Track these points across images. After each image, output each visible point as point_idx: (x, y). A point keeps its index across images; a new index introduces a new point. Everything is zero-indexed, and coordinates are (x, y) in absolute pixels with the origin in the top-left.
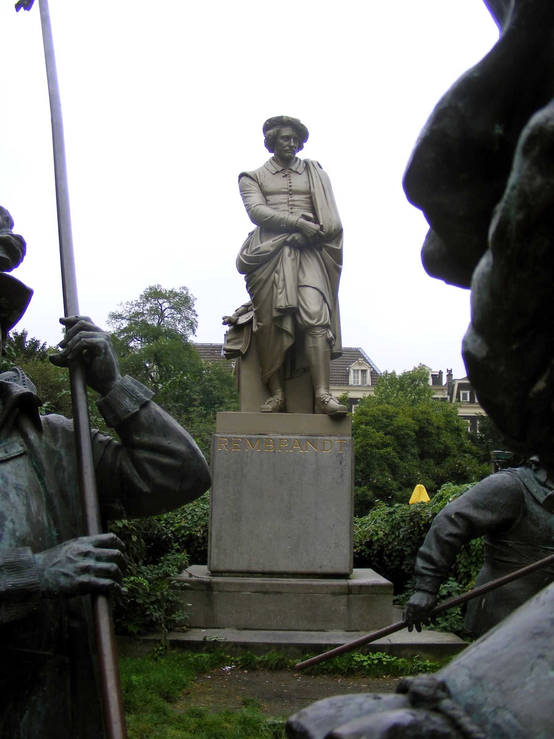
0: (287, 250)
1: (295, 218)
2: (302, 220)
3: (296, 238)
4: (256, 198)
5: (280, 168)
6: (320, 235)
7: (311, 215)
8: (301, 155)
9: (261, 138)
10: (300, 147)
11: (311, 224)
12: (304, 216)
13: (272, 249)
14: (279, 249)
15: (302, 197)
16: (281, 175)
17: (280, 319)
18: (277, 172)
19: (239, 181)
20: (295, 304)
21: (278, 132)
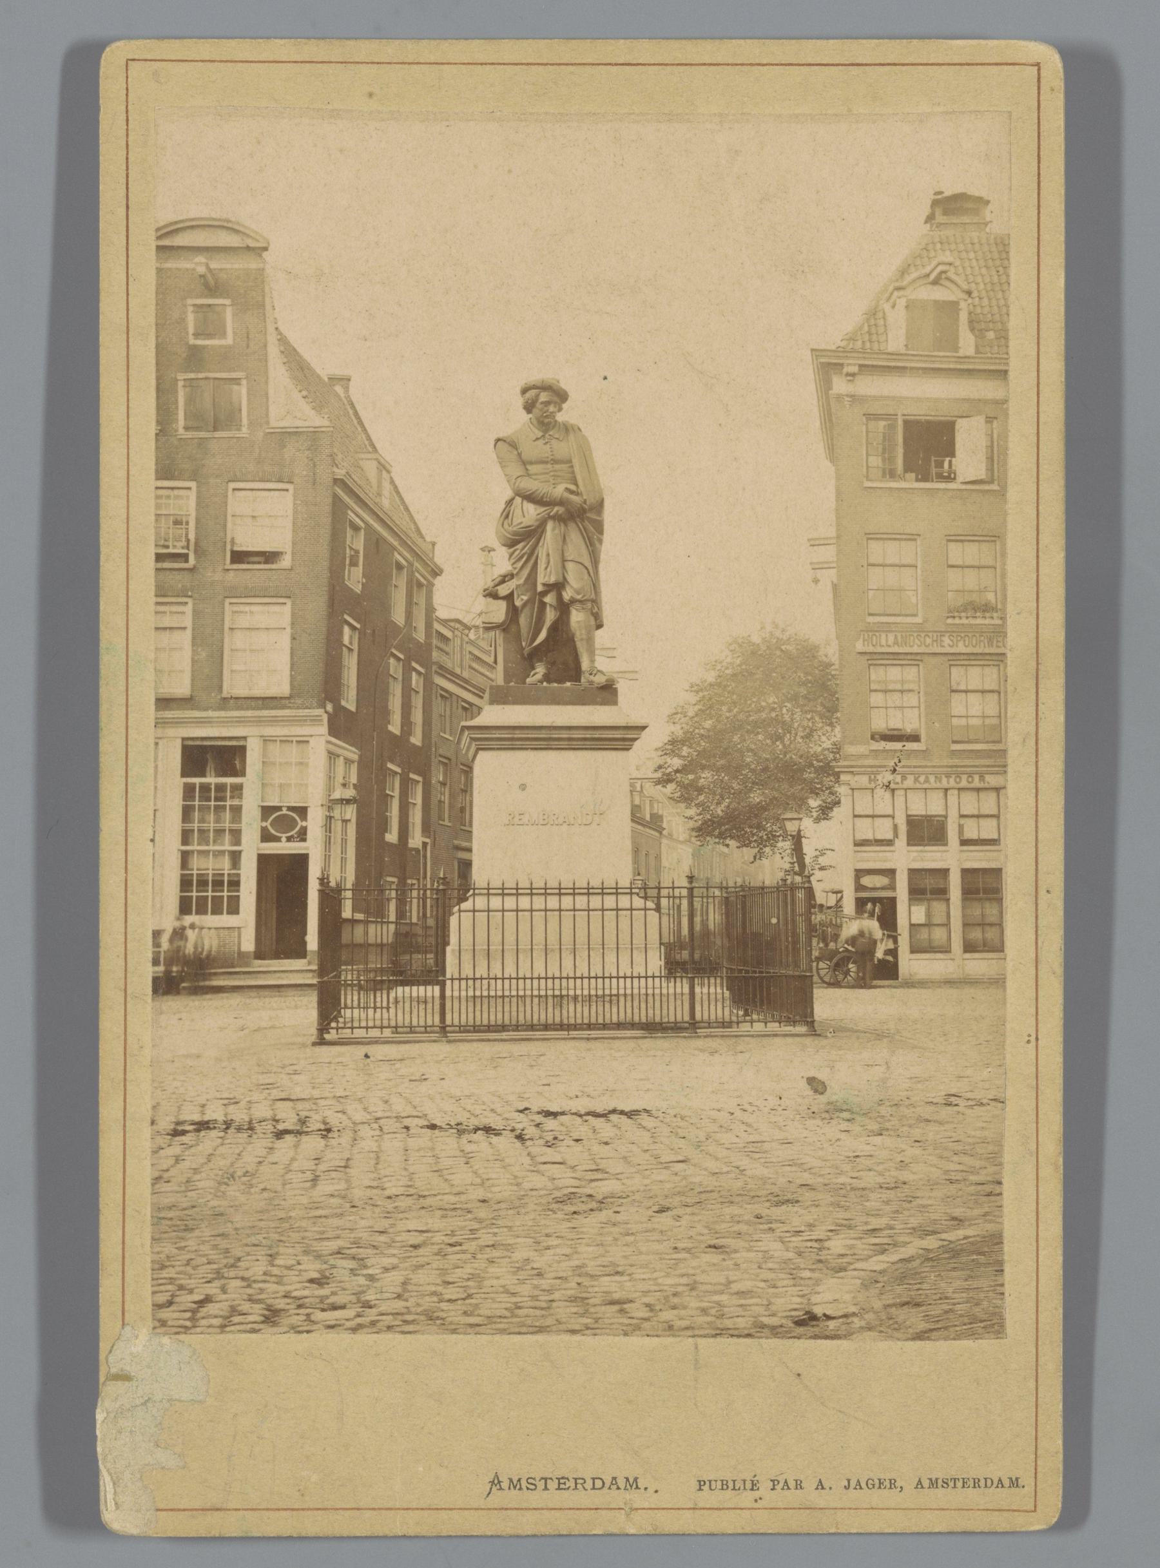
0: (550, 525)
1: (559, 491)
2: (566, 495)
3: (560, 512)
4: (516, 470)
5: (540, 434)
6: (582, 507)
7: (573, 487)
8: (560, 417)
9: (519, 401)
10: (560, 410)
11: (573, 497)
12: (567, 489)
13: (537, 524)
14: (542, 525)
15: (564, 466)
16: (541, 442)
17: (544, 594)
18: (537, 439)
19: (495, 446)
20: (561, 580)
21: (537, 396)
